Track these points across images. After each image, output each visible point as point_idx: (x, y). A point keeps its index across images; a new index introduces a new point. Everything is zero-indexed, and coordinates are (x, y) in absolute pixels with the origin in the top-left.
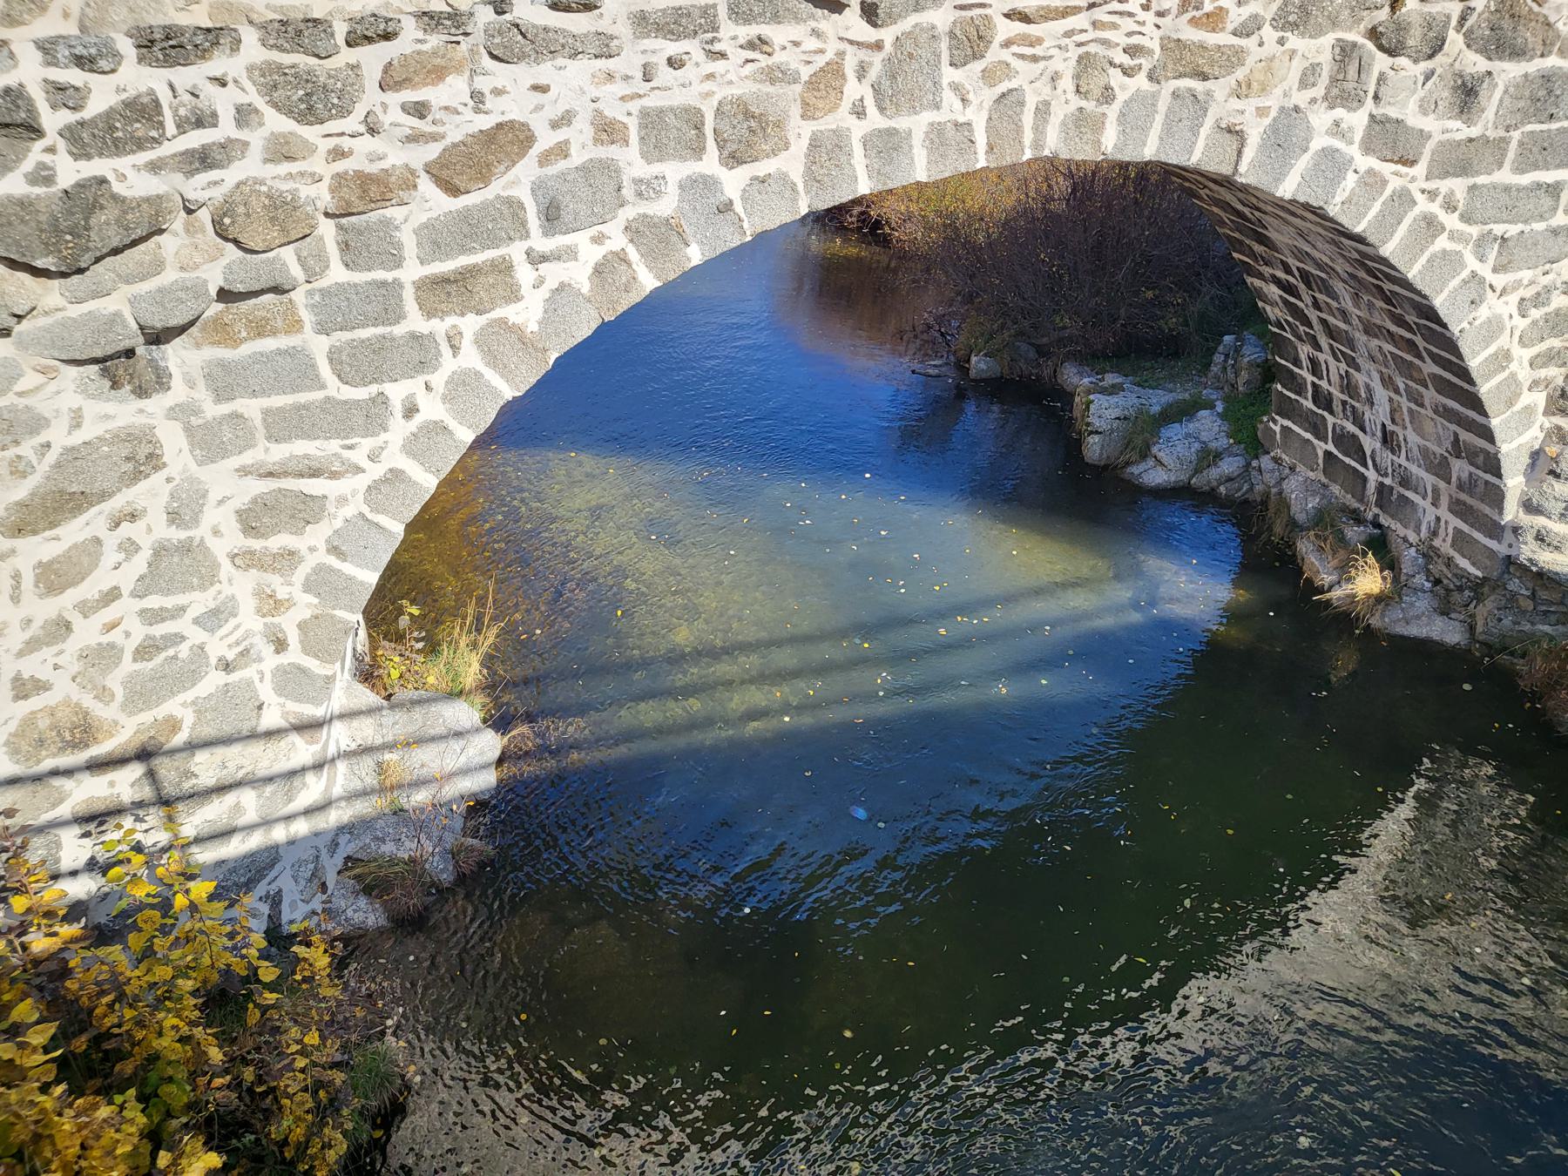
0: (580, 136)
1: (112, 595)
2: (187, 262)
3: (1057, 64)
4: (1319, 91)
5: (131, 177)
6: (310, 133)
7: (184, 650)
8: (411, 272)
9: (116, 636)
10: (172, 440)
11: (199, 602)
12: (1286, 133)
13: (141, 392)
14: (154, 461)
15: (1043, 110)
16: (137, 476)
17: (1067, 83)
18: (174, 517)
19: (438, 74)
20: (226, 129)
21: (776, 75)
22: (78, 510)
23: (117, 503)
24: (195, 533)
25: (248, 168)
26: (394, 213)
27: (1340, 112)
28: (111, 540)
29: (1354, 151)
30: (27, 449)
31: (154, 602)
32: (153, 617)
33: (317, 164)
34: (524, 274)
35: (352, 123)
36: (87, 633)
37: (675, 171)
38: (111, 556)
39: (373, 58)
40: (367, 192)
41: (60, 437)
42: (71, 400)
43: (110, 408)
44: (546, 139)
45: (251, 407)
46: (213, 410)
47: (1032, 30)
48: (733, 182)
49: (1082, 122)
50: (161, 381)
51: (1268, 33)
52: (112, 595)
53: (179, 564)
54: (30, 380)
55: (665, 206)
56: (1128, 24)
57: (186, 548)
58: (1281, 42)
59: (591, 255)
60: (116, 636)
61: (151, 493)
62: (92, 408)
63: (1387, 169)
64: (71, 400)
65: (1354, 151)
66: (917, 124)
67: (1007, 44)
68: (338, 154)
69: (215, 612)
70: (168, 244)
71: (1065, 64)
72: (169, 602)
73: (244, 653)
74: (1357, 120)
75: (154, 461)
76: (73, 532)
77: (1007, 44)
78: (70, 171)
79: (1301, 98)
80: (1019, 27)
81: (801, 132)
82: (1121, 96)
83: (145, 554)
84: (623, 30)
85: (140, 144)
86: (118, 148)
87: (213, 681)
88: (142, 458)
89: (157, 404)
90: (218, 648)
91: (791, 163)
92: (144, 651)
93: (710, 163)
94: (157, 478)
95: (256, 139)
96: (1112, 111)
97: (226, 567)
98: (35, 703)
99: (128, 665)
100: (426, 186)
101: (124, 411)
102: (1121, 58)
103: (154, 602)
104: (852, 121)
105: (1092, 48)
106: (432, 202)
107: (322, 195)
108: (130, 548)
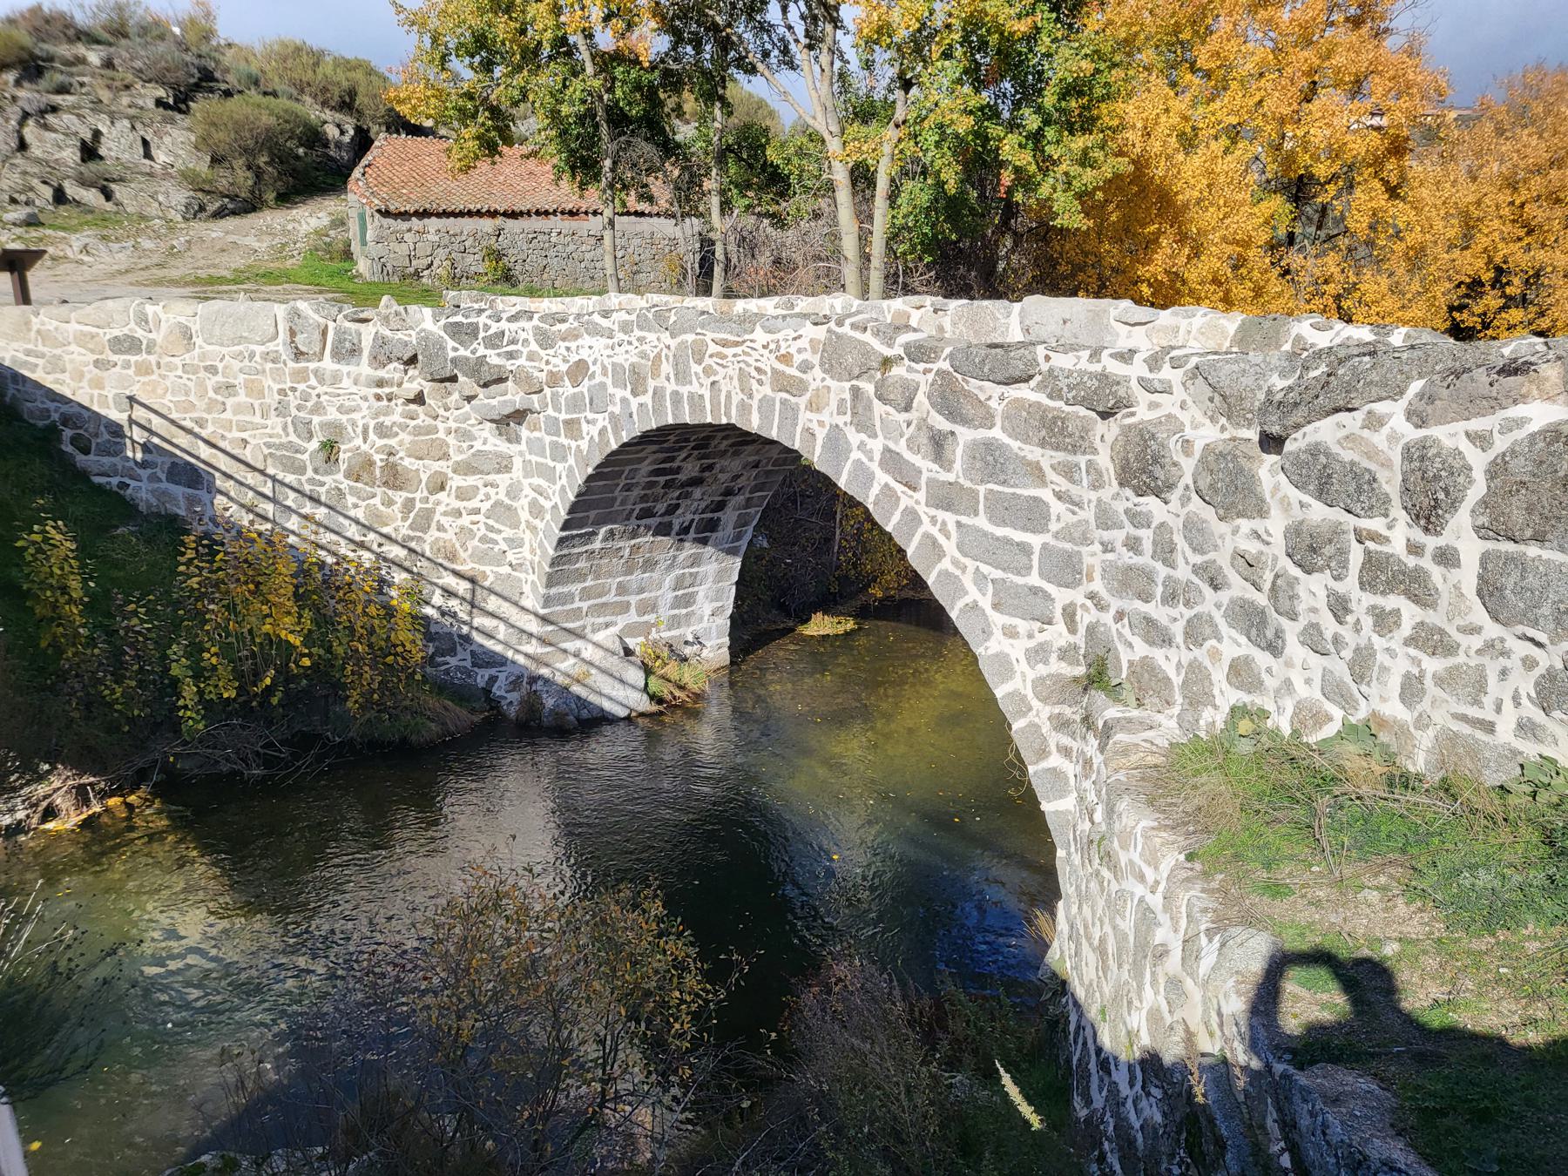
0: (597, 369)
1: (477, 511)
2: (512, 396)
3: (730, 371)
4: (848, 418)
5: (494, 358)
6: (542, 353)
7: (497, 548)
8: (563, 416)
9: (474, 527)
10: (517, 463)
11: (508, 532)
12: (835, 438)
13: (509, 441)
14: (507, 469)
15: (729, 396)
16: (499, 472)
17: (736, 382)
18: (508, 494)
19: (576, 337)
20: (519, 347)
21: (643, 355)
22: (474, 473)
23: (490, 478)
24: (515, 504)
25: (522, 361)
26: (560, 390)
27: (863, 436)
28: (483, 491)
29: (874, 466)
30: (465, 445)
31: (490, 522)
32: (490, 529)
33: (543, 366)
34: (584, 426)
35: (551, 352)
36: (466, 520)
37: (619, 393)
38: (481, 496)
39: (563, 327)
40: (554, 380)
41: (478, 445)
42: (486, 434)
43: (498, 442)
44: (592, 368)
45: (534, 458)
46: (528, 457)
47: (725, 351)
48: (634, 403)
49: (744, 408)
50: (518, 440)
51: (817, 372)
52: (477, 511)
53: (503, 512)
54: (473, 421)
55: (617, 409)
56: (755, 355)
57: (509, 508)
58: (823, 380)
59: (600, 425)
60: (474, 527)
61: (503, 480)
62: (492, 440)
63: (899, 488)
64: (486, 434)
65: (874, 466)
66: (685, 390)
67: (711, 356)
68: (548, 363)
69: (512, 540)
70: (510, 383)
71: (733, 371)
72: (497, 526)
73: (521, 565)
74: (876, 445)
75: (507, 469)
76: (472, 480)
77: (711, 356)
78: (481, 351)
79: (840, 420)
80: (719, 349)
81: (651, 384)
82: (757, 397)
83: (491, 502)
84: (616, 327)
85: (498, 347)
86: (494, 346)
87: (506, 570)
88: (504, 466)
89: (513, 449)
90: (510, 556)
91: (647, 399)
92: (483, 540)
93: (627, 394)
94: (507, 476)
95: (525, 351)
96: (755, 404)
97: (523, 526)
98: (441, 535)
99: (476, 542)
100: (567, 382)
101: (503, 446)
102: (754, 373)
103: (490, 522)
104: (666, 384)
105: (742, 365)
106: (567, 389)
107: (543, 376)
108: (488, 497)
